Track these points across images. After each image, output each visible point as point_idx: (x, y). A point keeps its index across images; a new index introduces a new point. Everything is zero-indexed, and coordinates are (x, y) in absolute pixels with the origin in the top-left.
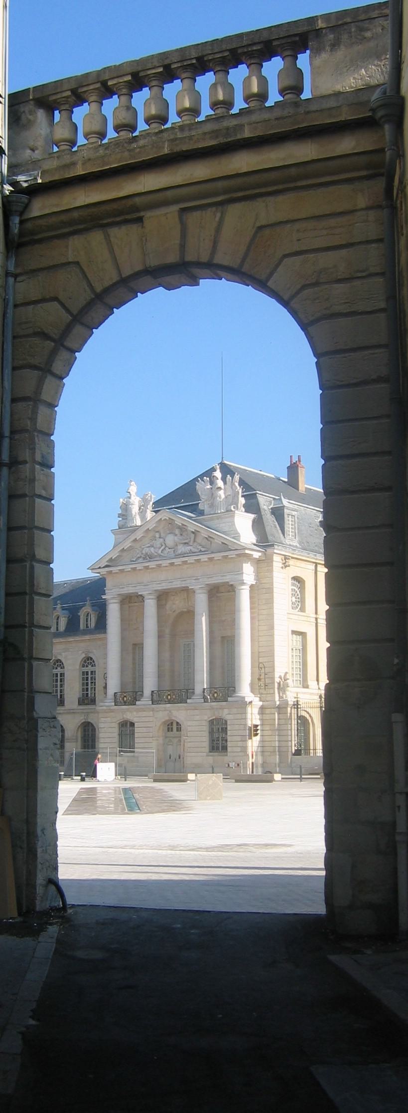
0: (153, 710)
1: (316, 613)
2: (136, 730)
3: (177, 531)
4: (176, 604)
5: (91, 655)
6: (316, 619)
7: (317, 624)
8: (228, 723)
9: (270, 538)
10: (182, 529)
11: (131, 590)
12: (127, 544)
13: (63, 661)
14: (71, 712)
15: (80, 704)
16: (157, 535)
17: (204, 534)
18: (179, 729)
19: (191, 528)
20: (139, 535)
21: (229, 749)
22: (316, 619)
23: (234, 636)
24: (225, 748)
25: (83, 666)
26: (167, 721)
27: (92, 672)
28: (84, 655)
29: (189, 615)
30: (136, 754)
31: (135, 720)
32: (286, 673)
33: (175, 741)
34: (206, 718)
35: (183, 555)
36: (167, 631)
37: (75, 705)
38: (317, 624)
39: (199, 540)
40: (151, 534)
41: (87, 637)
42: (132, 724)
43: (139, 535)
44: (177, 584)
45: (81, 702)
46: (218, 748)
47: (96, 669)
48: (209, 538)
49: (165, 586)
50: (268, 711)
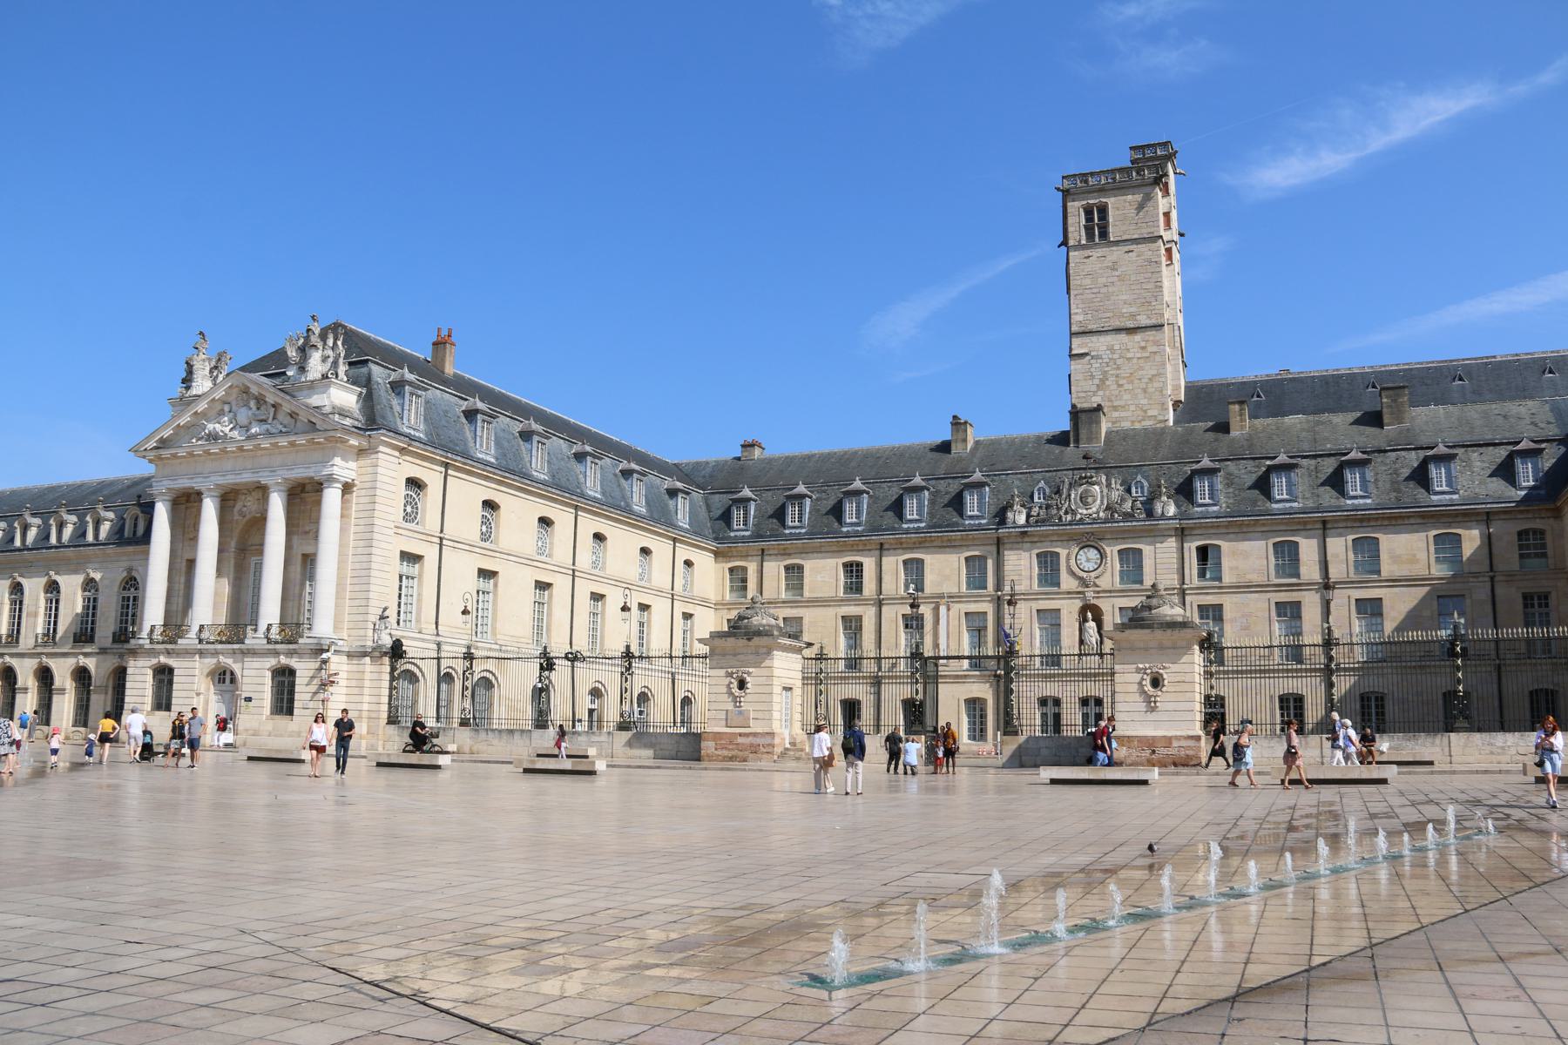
2: (175, 679)
3: (252, 404)
4: (249, 504)
5: (134, 574)
7: (441, 545)
9: (379, 420)
10: (260, 400)
11: (184, 483)
12: (185, 419)
16: (226, 408)
17: (286, 407)
18: (233, 680)
19: (270, 399)
20: (202, 406)
21: (296, 711)
23: (315, 555)
29: (259, 523)
32: (385, 609)
35: (254, 436)
36: (233, 544)
37: (108, 642)
38: (441, 545)
39: (280, 416)
40: (218, 406)
41: (130, 549)
43: (202, 406)
44: (247, 477)
48: (293, 415)
49: (230, 479)
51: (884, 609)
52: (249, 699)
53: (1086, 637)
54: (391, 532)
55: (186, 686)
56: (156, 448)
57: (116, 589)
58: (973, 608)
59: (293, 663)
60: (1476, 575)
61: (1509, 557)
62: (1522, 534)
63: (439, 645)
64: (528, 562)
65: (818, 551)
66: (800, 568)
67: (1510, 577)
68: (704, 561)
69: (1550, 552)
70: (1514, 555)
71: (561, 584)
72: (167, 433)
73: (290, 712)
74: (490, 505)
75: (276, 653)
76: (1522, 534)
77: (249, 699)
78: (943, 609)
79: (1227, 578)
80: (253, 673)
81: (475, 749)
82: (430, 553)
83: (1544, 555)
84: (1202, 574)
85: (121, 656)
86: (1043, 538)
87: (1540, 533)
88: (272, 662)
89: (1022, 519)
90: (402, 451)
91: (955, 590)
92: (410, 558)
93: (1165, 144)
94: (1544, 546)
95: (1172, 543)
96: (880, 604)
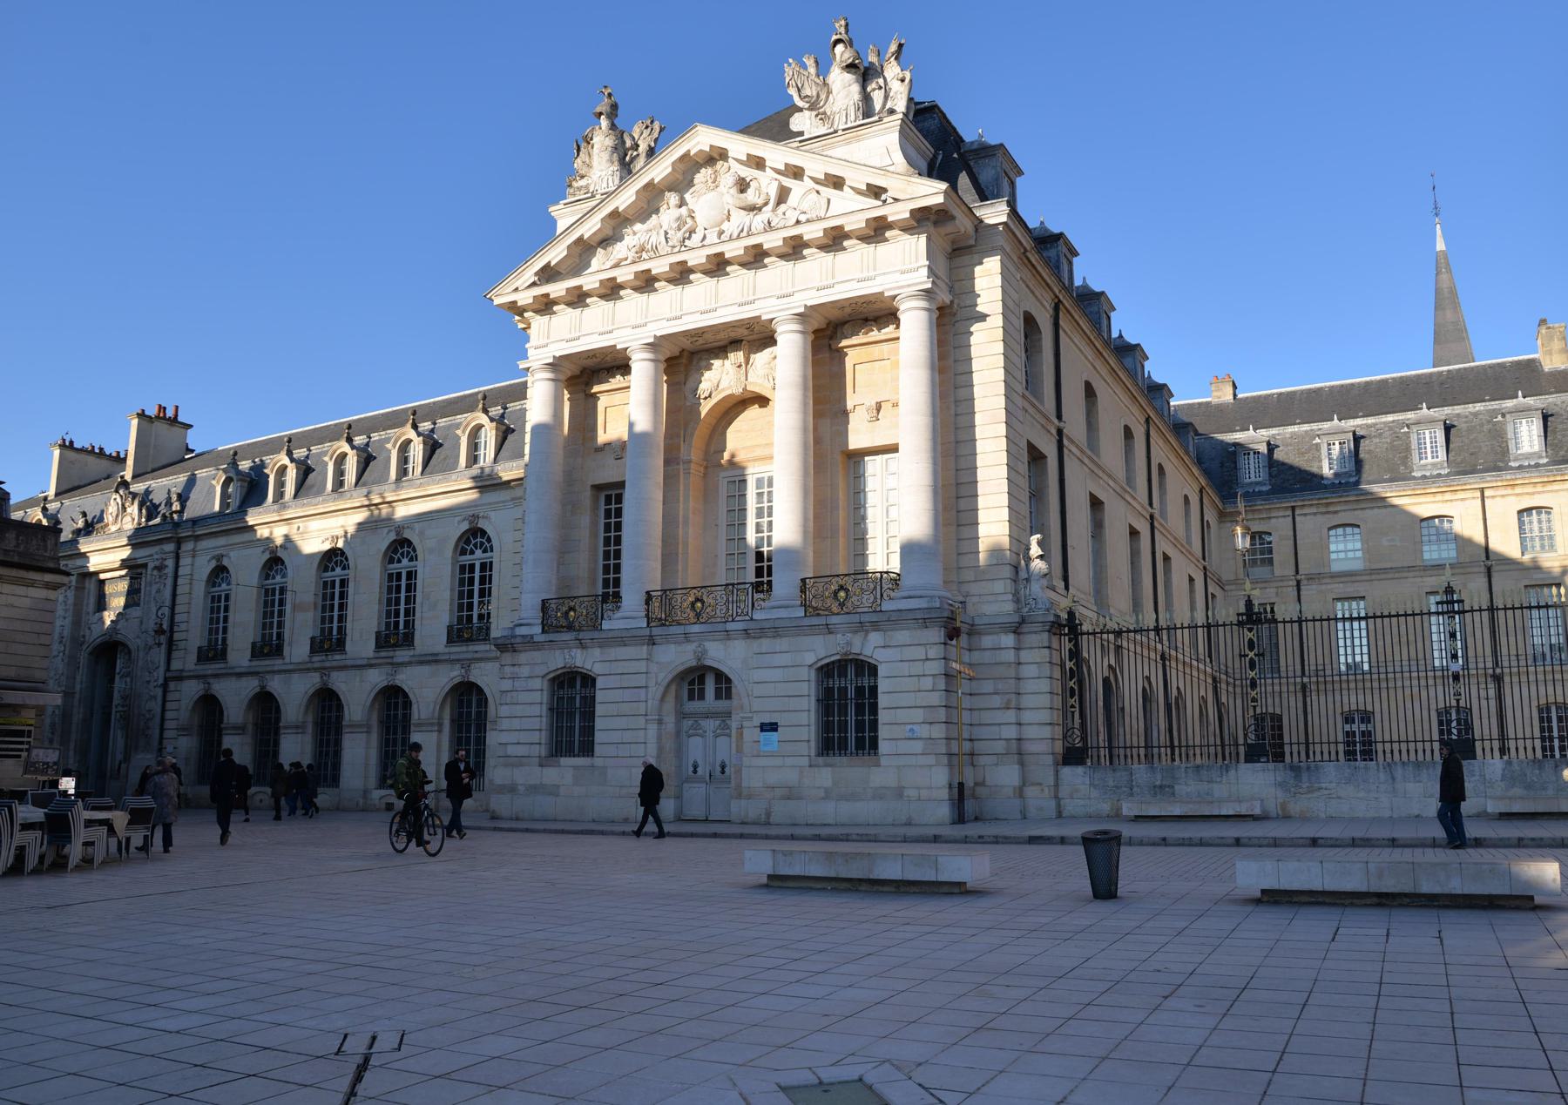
0: (652, 641)
1: (1059, 417)
2: (600, 696)
8: (881, 671)
13: (415, 541)
14: (432, 660)
15: (450, 641)
21: (883, 747)
24: (874, 745)
25: (463, 552)
26: (690, 670)
27: (483, 566)
28: (465, 526)
30: (598, 762)
31: (597, 669)
33: (710, 725)
34: (810, 658)
42: (589, 681)
45: (458, 634)
46: (843, 747)
47: (495, 556)
50: (987, 641)
52: (772, 727)
55: (625, 708)
56: (534, 284)
57: (449, 551)
59: (871, 646)
72: (555, 254)
73: (867, 743)
75: (829, 630)
77: (772, 727)
80: (777, 674)
81: (1295, 808)
85: (467, 664)
88: (821, 649)
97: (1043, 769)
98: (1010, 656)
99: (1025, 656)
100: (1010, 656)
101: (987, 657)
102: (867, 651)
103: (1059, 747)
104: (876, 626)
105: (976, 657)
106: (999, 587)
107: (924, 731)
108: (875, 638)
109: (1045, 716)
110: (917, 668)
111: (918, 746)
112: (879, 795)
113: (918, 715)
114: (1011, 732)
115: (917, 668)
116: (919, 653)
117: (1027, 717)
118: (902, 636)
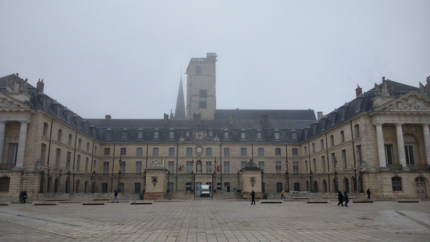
6: (50, 140)
8: (11, 179)
21: (10, 190)
22: (50, 140)
50: (29, 175)
51: (148, 160)
53: (198, 168)
54: (40, 138)
58: (171, 160)
60: (284, 158)
61: (290, 155)
62: (293, 149)
63: (49, 170)
64: (66, 147)
65: (130, 144)
66: (125, 149)
67: (290, 158)
68: (98, 146)
69: (298, 153)
70: (291, 153)
71: (72, 152)
74: (60, 131)
76: (293, 149)
78: (163, 160)
79: (231, 155)
82: (47, 144)
83: (297, 154)
84: (225, 154)
86: (188, 144)
87: (296, 149)
89: (183, 140)
90: (44, 115)
91: (166, 156)
92: (44, 145)
93: (215, 54)
94: (297, 152)
95: (218, 147)
96: (147, 159)
97: (36, 194)
98: (33, 177)
99: (35, 177)
100: (33, 177)
101: (29, 177)
102: (9, 176)
103: (39, 190)
104: (11, 172)
105: (27, 177)
106: (32, 166)
107: (16, 188)
108: (10, 174)
109: (37, 186)
110: (16, 179)
111: (15, 190)
112: (8, 197)
113: (16, 185)
114: (32, 188)
115: (16, 179)
116: (17, 176)
117: (35, 186)
118: (14, 174)
